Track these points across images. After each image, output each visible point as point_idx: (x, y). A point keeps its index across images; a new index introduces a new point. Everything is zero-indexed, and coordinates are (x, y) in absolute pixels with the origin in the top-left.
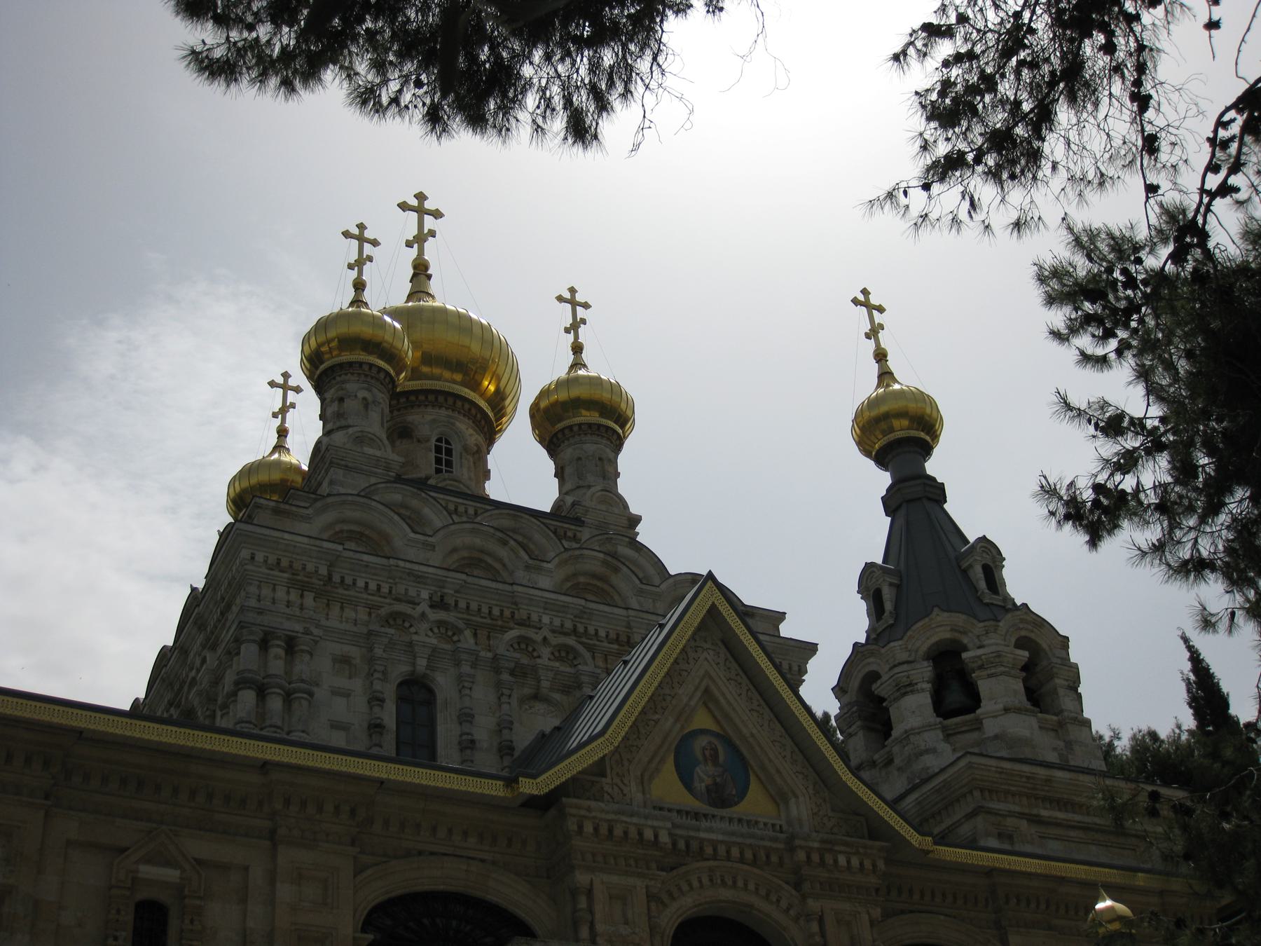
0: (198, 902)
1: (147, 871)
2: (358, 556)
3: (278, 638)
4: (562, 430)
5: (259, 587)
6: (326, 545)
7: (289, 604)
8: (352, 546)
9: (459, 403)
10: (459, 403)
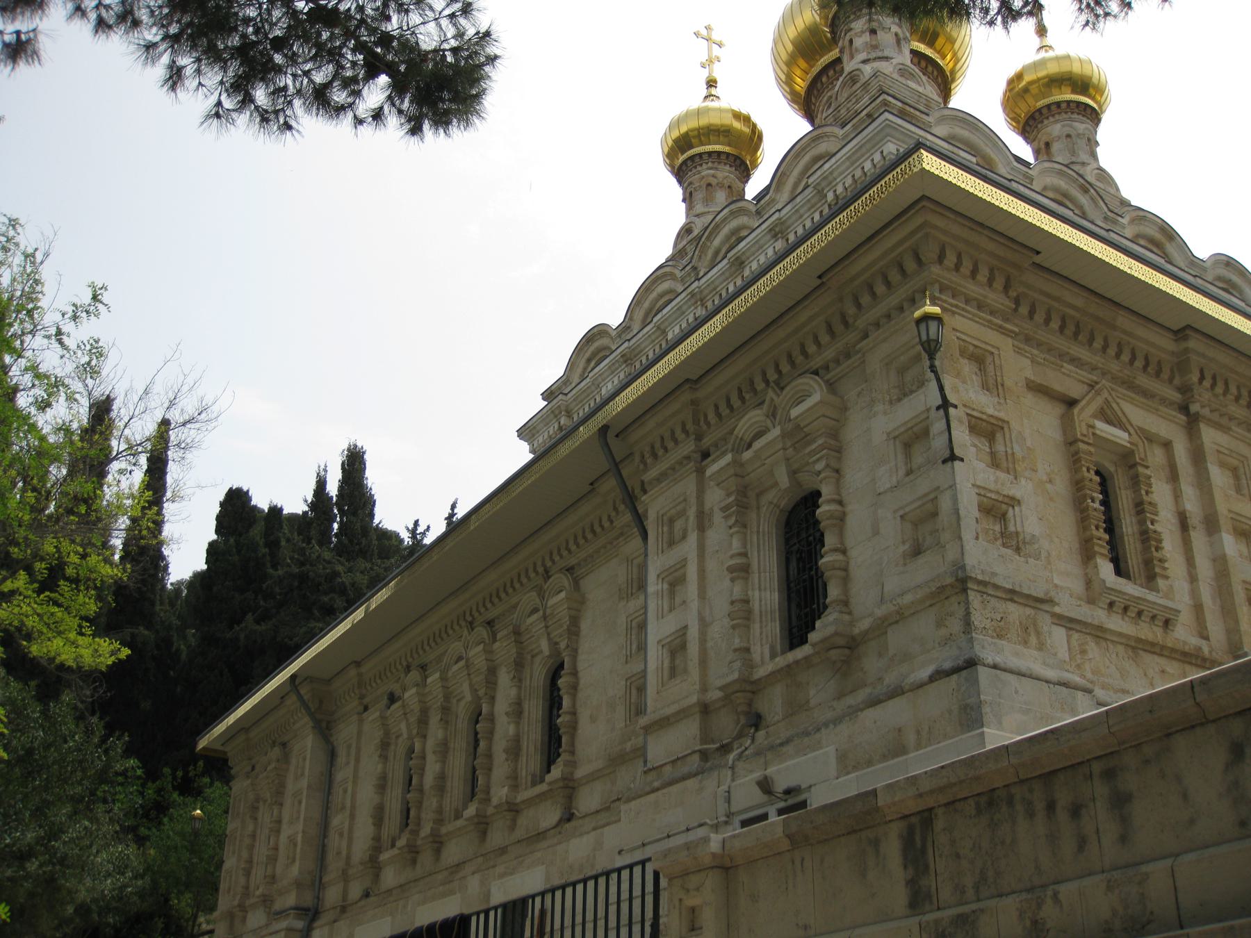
4: (1048, 106)
9: (930, 69)
10: (930, 69)
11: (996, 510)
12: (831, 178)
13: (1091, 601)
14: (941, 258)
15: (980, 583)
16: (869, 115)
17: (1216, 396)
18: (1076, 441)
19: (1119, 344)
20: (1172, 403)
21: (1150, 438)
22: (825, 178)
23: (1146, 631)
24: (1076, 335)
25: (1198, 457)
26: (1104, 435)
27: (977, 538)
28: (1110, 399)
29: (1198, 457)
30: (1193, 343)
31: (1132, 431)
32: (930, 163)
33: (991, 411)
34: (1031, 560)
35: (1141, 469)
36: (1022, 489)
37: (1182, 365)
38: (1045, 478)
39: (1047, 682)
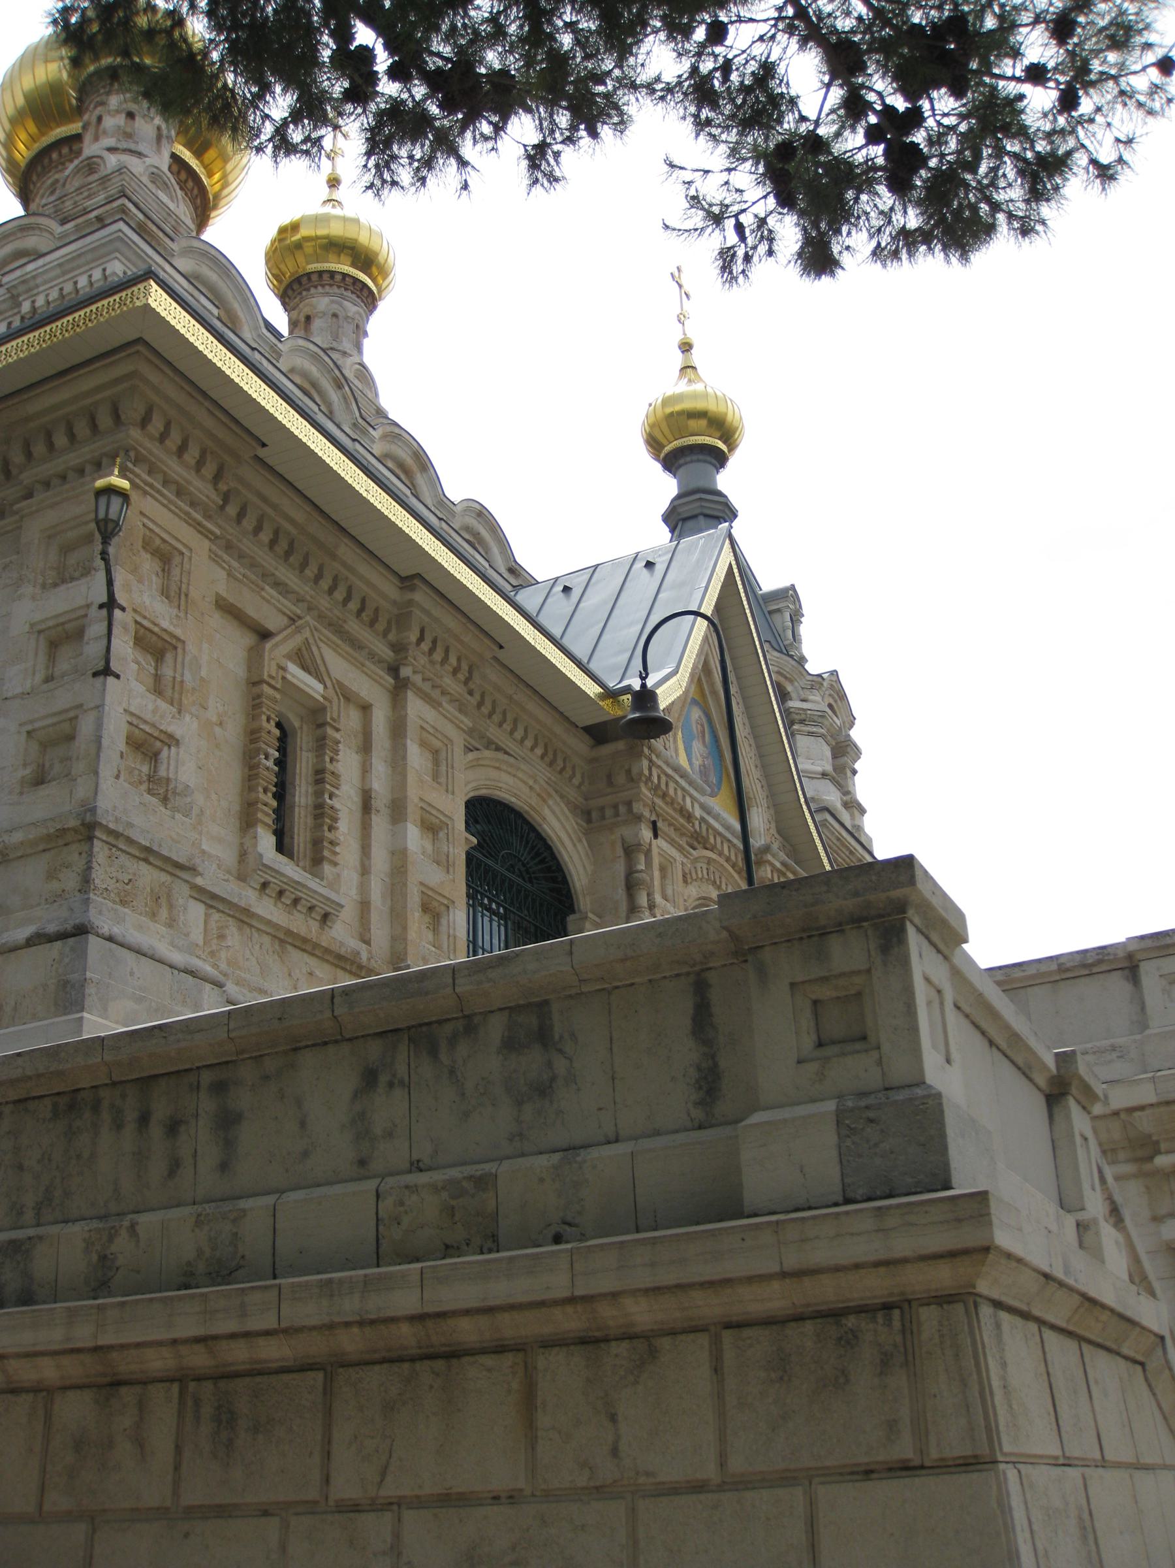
4: (320, 273)
9: (190, 184)
11: (148, 746)
12: (32, 284)
13: (242, 878)
14: (145, 422)
16: (99, 219)
17: (432, 662)
18: (262, 681)
19: (335, 579)
21: (347, 696)
22: (24, 282)
23: (299, 923)
24: (288, 554)
25: (398, 730)
26: (295, 681)
27: (117, 777)
28: (311, 641)
29: (398, 730)
30: (418, 596)
31: (329, 684)
32: (158, 300)
33: (165, 624)
34: (178, 816)
35: (330, 731)
36: (185, 727)
37: (401, 619)
38: (214, 719)
39: (171, 967)
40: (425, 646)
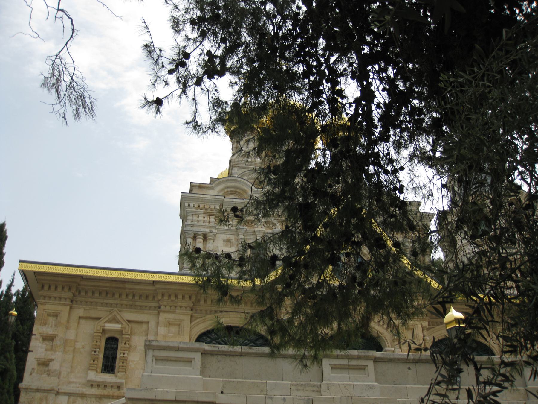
0: (127, 336)
1: (109, 326)
2: (231, 200)
3: (200, 235)
5: (192, 217)
6: (217, 197)
7: (204, 222)
8: (233, 196)
11: (44, 363)
15: (25, 389)
17: (172, 301)
20: (155, 307)
23: (105, 392)
27: (31, 374)
30: (158, 286)
31: (124, 323)
40: (166, 298)
